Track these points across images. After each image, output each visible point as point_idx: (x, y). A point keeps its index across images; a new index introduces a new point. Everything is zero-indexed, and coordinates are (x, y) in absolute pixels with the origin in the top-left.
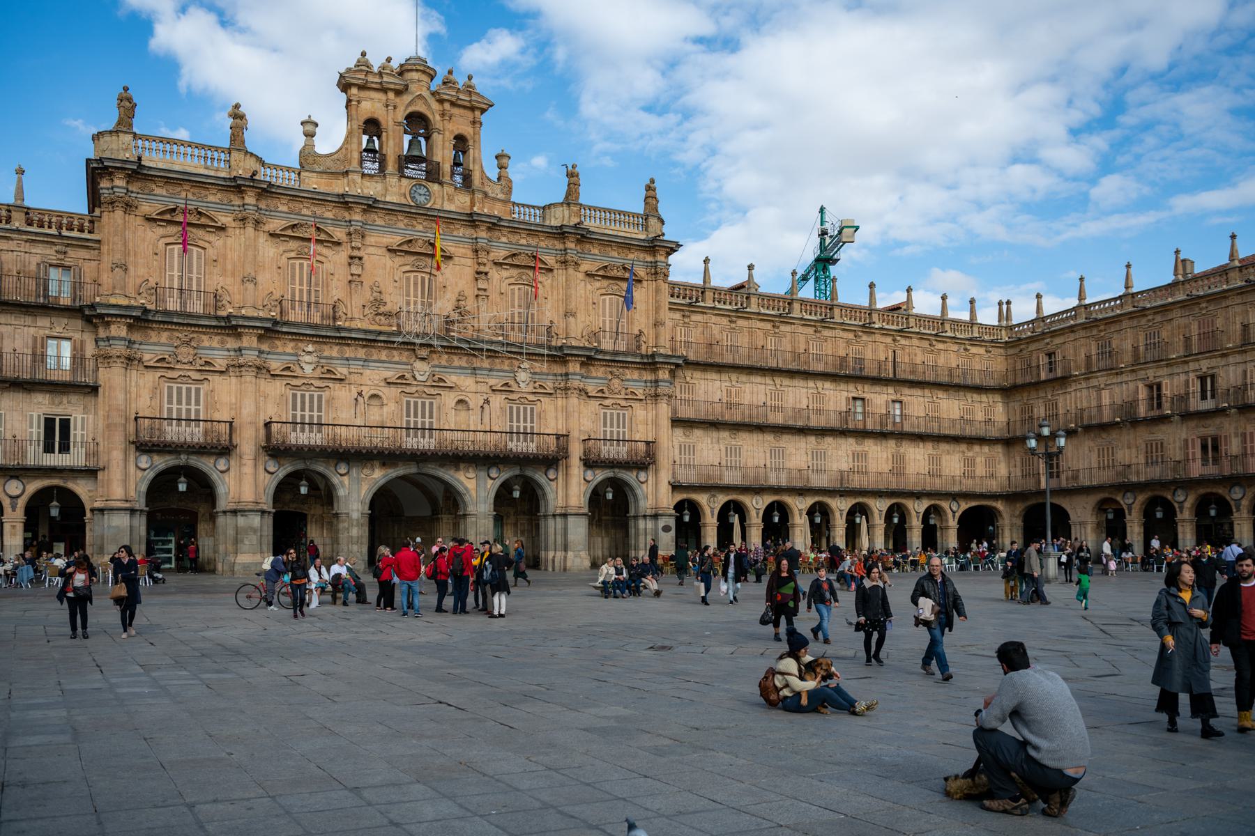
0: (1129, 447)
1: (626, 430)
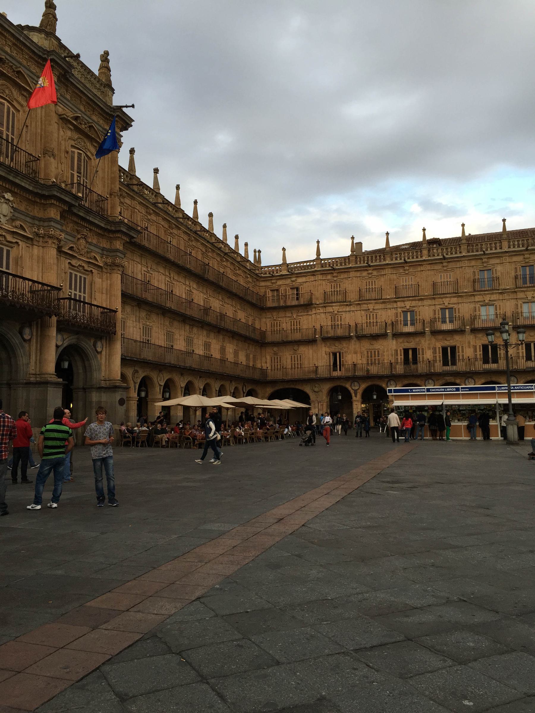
0: (356, 353)
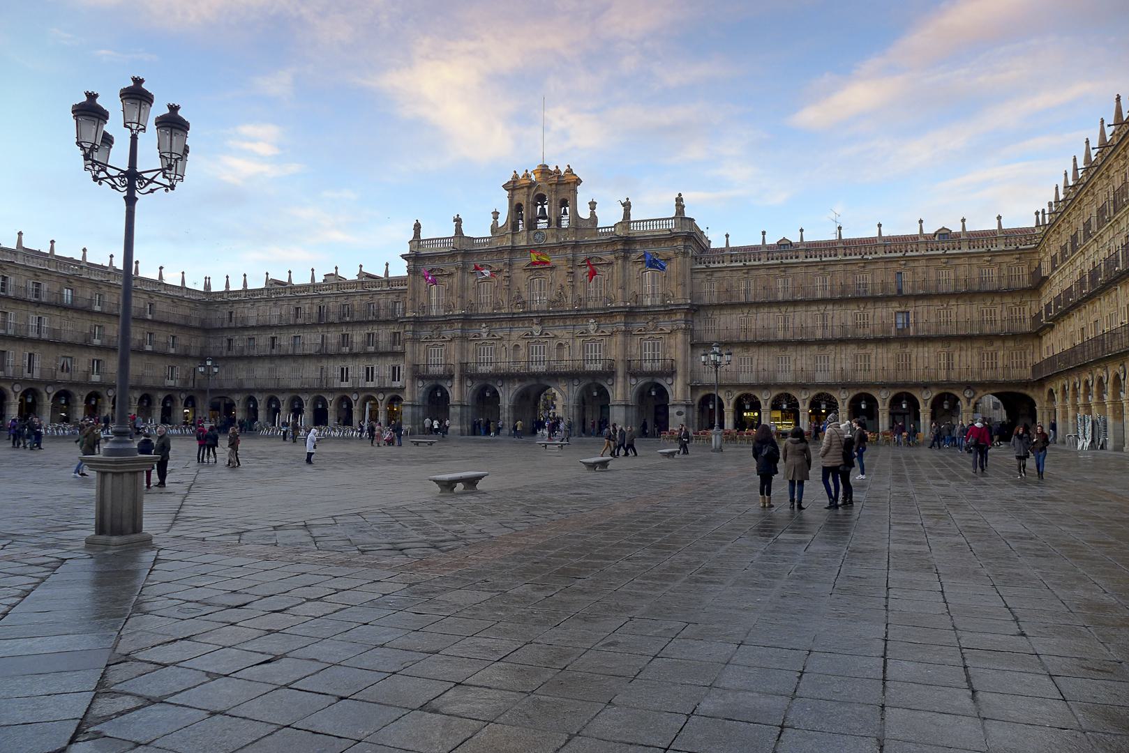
1: (660, 352)
